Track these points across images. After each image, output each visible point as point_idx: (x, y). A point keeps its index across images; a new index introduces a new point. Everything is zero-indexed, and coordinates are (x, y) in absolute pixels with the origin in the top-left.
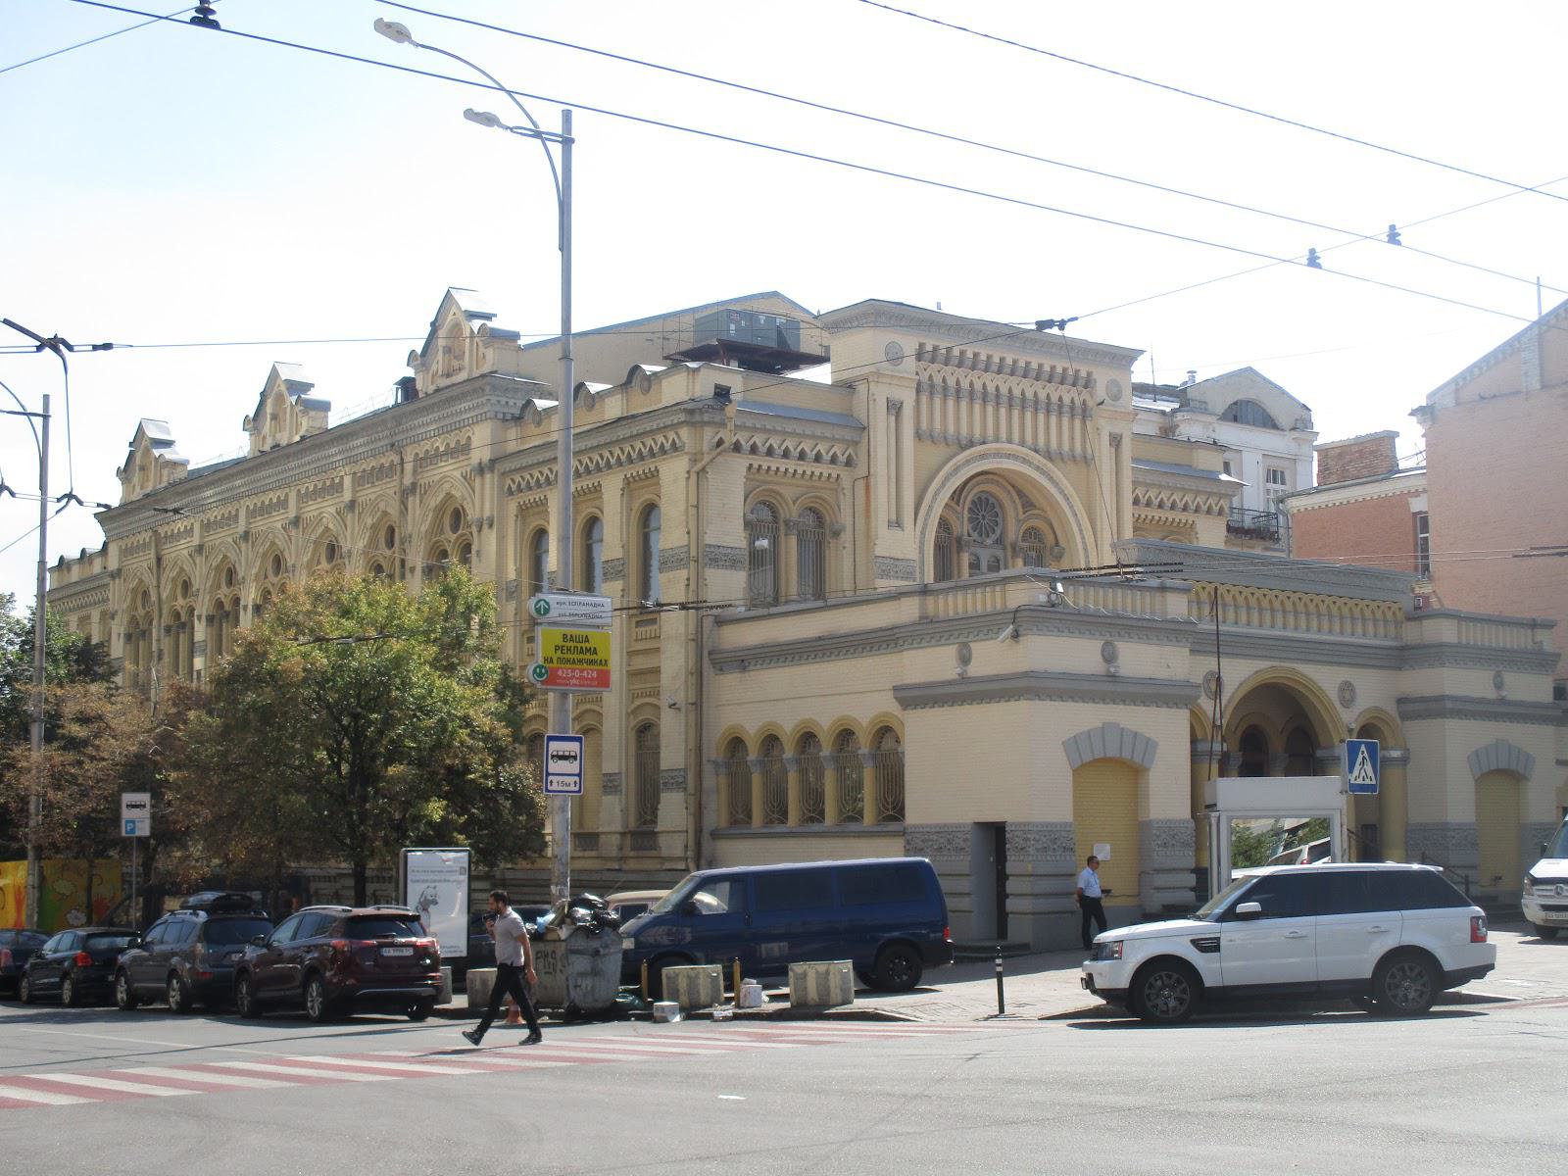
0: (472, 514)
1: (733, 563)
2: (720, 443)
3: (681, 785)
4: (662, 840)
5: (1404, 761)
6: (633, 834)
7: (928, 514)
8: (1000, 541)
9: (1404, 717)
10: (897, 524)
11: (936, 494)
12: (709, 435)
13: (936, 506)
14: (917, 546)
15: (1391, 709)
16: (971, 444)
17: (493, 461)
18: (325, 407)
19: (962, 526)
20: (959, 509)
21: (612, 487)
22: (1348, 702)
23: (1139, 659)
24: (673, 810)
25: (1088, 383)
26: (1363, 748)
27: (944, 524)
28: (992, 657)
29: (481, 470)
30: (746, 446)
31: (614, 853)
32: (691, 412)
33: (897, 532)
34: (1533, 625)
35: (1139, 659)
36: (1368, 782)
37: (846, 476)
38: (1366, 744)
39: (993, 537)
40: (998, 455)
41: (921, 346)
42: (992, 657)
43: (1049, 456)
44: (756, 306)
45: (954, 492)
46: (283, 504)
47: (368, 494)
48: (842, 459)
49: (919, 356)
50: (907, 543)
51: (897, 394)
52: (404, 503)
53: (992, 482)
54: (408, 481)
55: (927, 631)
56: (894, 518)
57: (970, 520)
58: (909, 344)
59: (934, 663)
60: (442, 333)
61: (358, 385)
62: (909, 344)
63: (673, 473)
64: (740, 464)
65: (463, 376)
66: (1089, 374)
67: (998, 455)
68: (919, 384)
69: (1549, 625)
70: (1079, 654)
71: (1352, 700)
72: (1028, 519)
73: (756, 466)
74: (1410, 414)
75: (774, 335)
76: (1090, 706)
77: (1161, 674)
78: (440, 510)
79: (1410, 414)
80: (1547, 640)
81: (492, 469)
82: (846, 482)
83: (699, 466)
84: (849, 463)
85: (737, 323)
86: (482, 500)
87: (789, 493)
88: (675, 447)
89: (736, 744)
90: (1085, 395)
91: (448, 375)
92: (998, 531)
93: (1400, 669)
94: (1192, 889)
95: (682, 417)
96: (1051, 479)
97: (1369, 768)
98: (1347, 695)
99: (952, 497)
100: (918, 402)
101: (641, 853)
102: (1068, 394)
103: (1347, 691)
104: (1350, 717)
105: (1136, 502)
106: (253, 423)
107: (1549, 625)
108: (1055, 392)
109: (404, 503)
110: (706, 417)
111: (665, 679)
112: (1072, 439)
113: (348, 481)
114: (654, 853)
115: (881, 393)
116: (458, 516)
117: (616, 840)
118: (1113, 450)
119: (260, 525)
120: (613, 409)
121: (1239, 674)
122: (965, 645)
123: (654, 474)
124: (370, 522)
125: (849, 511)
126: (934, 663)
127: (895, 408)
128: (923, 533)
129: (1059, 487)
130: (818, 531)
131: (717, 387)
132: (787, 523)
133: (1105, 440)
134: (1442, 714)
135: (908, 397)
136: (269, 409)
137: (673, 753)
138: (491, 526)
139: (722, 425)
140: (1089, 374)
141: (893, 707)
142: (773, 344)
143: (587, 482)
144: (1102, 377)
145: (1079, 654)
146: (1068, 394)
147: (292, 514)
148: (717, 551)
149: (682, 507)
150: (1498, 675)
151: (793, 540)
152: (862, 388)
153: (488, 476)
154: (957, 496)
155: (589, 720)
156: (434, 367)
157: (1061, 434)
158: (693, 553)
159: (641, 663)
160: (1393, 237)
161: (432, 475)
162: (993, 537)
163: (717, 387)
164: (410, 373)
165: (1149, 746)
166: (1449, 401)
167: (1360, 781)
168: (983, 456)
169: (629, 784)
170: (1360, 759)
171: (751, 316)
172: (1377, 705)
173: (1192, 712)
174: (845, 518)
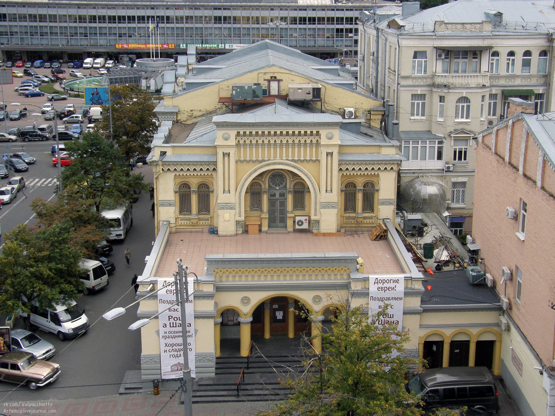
7: (243, 187)
10: (229, 191)
11: (246, 180)
16: (264, 161)
37: (214, 174)
39: (281, 186)
41: (238, 133)
56: (227, 189)
58: (232, 133)
62: (232, 133)
66: (318, 132)
72: (296, 179)
73: (178, 174)
75: (251, 92)
84: (214, 169)
85: (236, 91)
90: (317, 138)
96: (299, 170)
103: (317, 299)
118: (329, 158)
128: (240, 193)
135: (232, 151)
140: (318, 132)
144: (324, 132)
168: (268, 165)
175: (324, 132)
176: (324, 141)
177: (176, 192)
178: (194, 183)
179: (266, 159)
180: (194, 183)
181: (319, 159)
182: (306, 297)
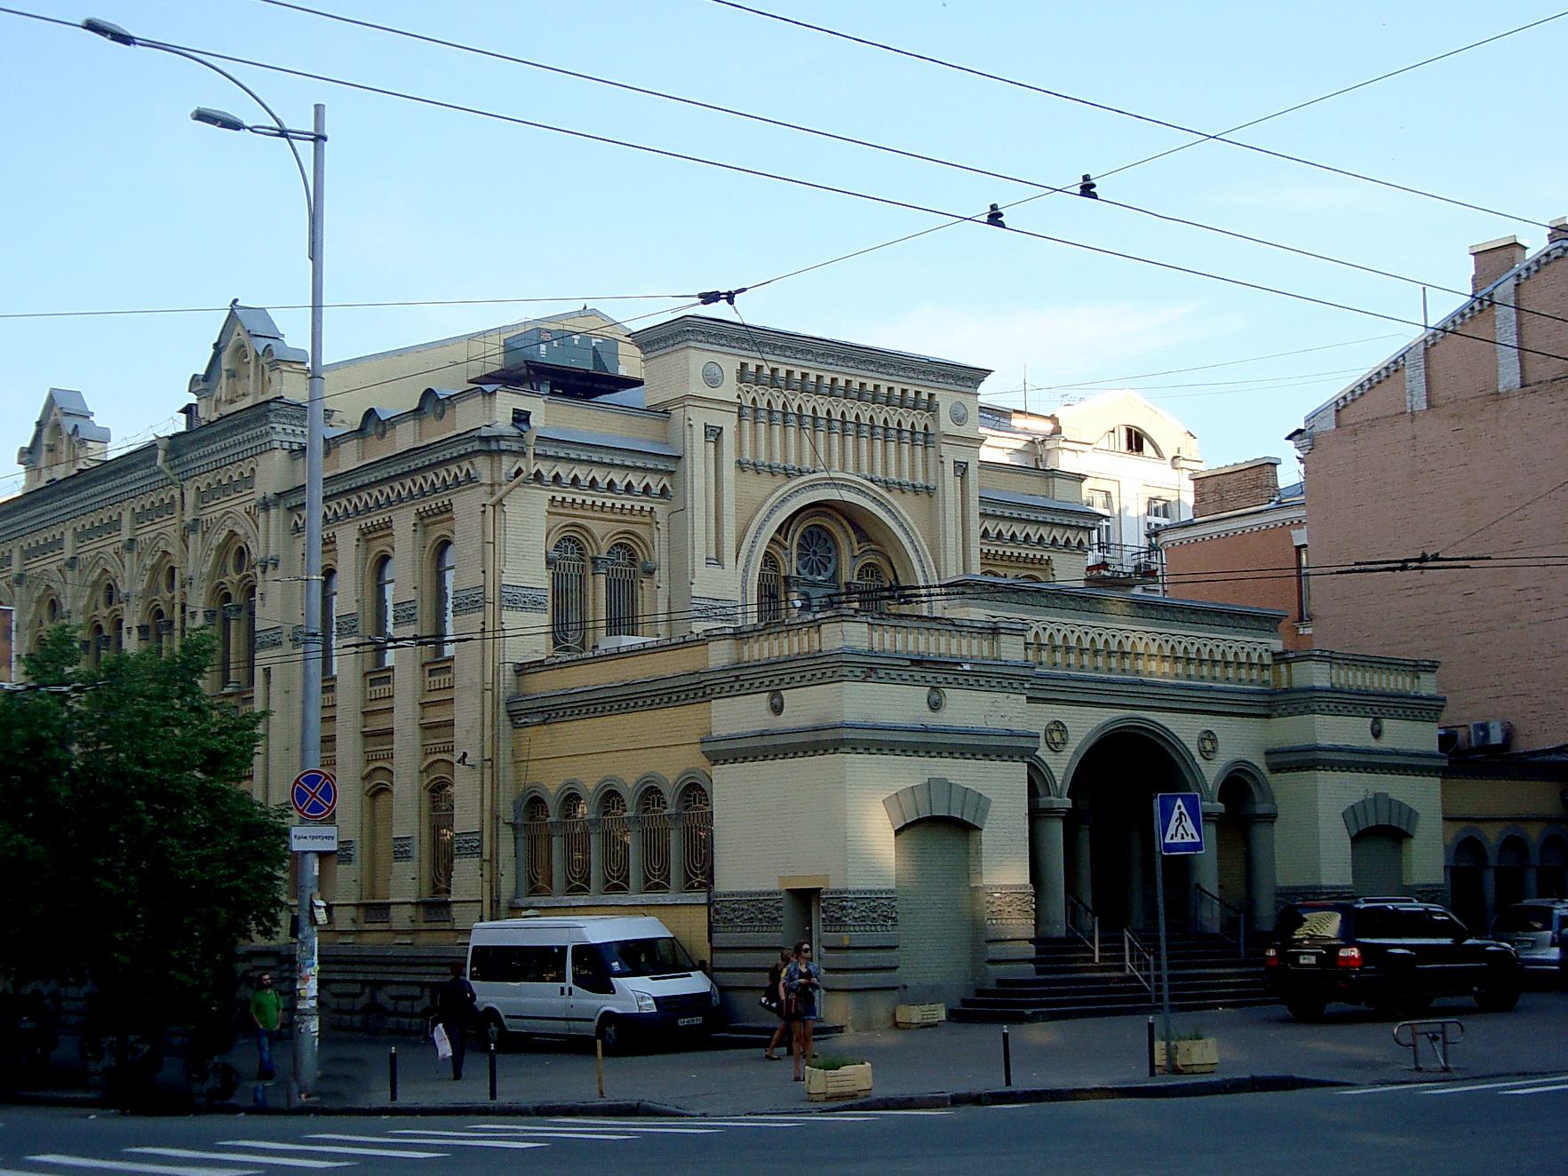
0: (257, 553)
1: (536, 605)
2: (519, 472)
3: (476, 851)
4: (455, 909)
5: (1271, 818)
6: (424, 904)
8: (834, 578)
9: (1275, 769)
10: (718, 561)
12: (507, 465)
13: (760, 540)
14: (739, 584)
15: (1260, 762)
17: (279, 495)
18: (104, 437)
19: (790, 565)
20: (787, 544)
21: (403, 521)
22: (1207, 755)
23: (968, 709)
24: (466, 878)
25: (931, 406)
26: (1179, 802)
27: (770, 560)
28: (806, 706)
29: (265, 505)
30: (548, 475)
31: (408, 926)
32: (487, 439)
33: (717, 569)
34: (1418, 668)
35: (968, 709)
36: (1188, 839)
37: (661, 510)
38: (1183, 798)
40: (831, 483)
41: (743, 365)
42: (806, 706)
43: (887, 485)
44: (580, 325)
45: (781, 526)
46: (58, 544)
47: (147, 533)
48: (656, 490)
49: (742, 374)
50: (729, 582)
51: (717, 419)
52: (184, 540)
53: (825, 514)
54: (188, 518)
55: (737, 681)
56: (713, 555)
57: (800, 556)
58: (730, 365)
59: (739, 715)
60: (225, 357)
61: (139, 409)
62: (730, 365)
63: (466, 504)
64: (541, 497)
65: (248, 402)
67: (831, 483)
68: (741, 407)
69: (1433, 667)
70: (900, 704)
71: (1214, 751)
74: (1289, 438)
76: (916, 760)
77: (995, 724)
78: (223, 548)
79: (1289, 438)
80: (1427, 685)
81: (277, 505)
82: (661, 510)
83: (495, 498)
86: (268, 536)
87: (598, 528)
88: (470, 478)
89: (534, 803)
91: (232, 402)
92: (831, 567)
93: (1267, 716)
94: (1030, 961)
95: (477, 446)
97: (1189, 825)
98: (1209, 746)
99: (779, 531)
100: (740, 426)
101: (433, 926)
102: (909, 419)
104: (1211, 773)
105: (985, 534)
106: (28, 456)
107: (1433, 667)
108: (894, 416)
109: (184, 540)
110: (504, 445)
111: (459, 733)
112: (785, 445)
113: (126, 517)
114: (448, 926)
115: (699, 418)
116: (242, 553)
117: (408, 911)
119: (36, 566)
120: (405, 438)
121: (1085, 724)
122: (776, 693)
123: (448, 509)
124: (149, 562)
125: (664, 543)
126: (739, 715)
127: (714, 434)
129: (901, 518)
130: (629, 565)
131: (516, 411)
132: (594, 560)
133: (949, 468)
134: (1311, 766)
135: (728, 422)
136: (45, 440)
137: (467, 817)
138: (276, 565)
139: (521, 453)
141: (701, 762)
142: (589, 366)
143: (376, 519)
144: (946, 400)
145: (900, 704)
146: (909, 419)
147: (68, 555)
148: (514, 591)
149: (478, 543)
150: (1376, 720)
151: (602, 579)
152: (677, 413)
153: (273, 512)
154: (784, 528)
155: (380, 779)
156: (217, 394)
157: (902, 462)
158: (489, 594)
159: (435, 715)
160: (1087, 189)
161: (214, 511)
162: (829, 574)
163: (516, 411)
164: (193, 399)
165: (982, 803)
166: (1329, 424)
167: (1177, 840)
169: (421, 850)
170: (1176, 812)
171: (565, 336)
172: (1243, 757)
173: (1030, 764)
174: (660, 556)
175: (946, 400)
176: (946, 425)
177: (550, 562)
178: (603, 533)
179: (807, 464)
180: (603, 533)
181: (931, 484)
182: (1185, 729)
